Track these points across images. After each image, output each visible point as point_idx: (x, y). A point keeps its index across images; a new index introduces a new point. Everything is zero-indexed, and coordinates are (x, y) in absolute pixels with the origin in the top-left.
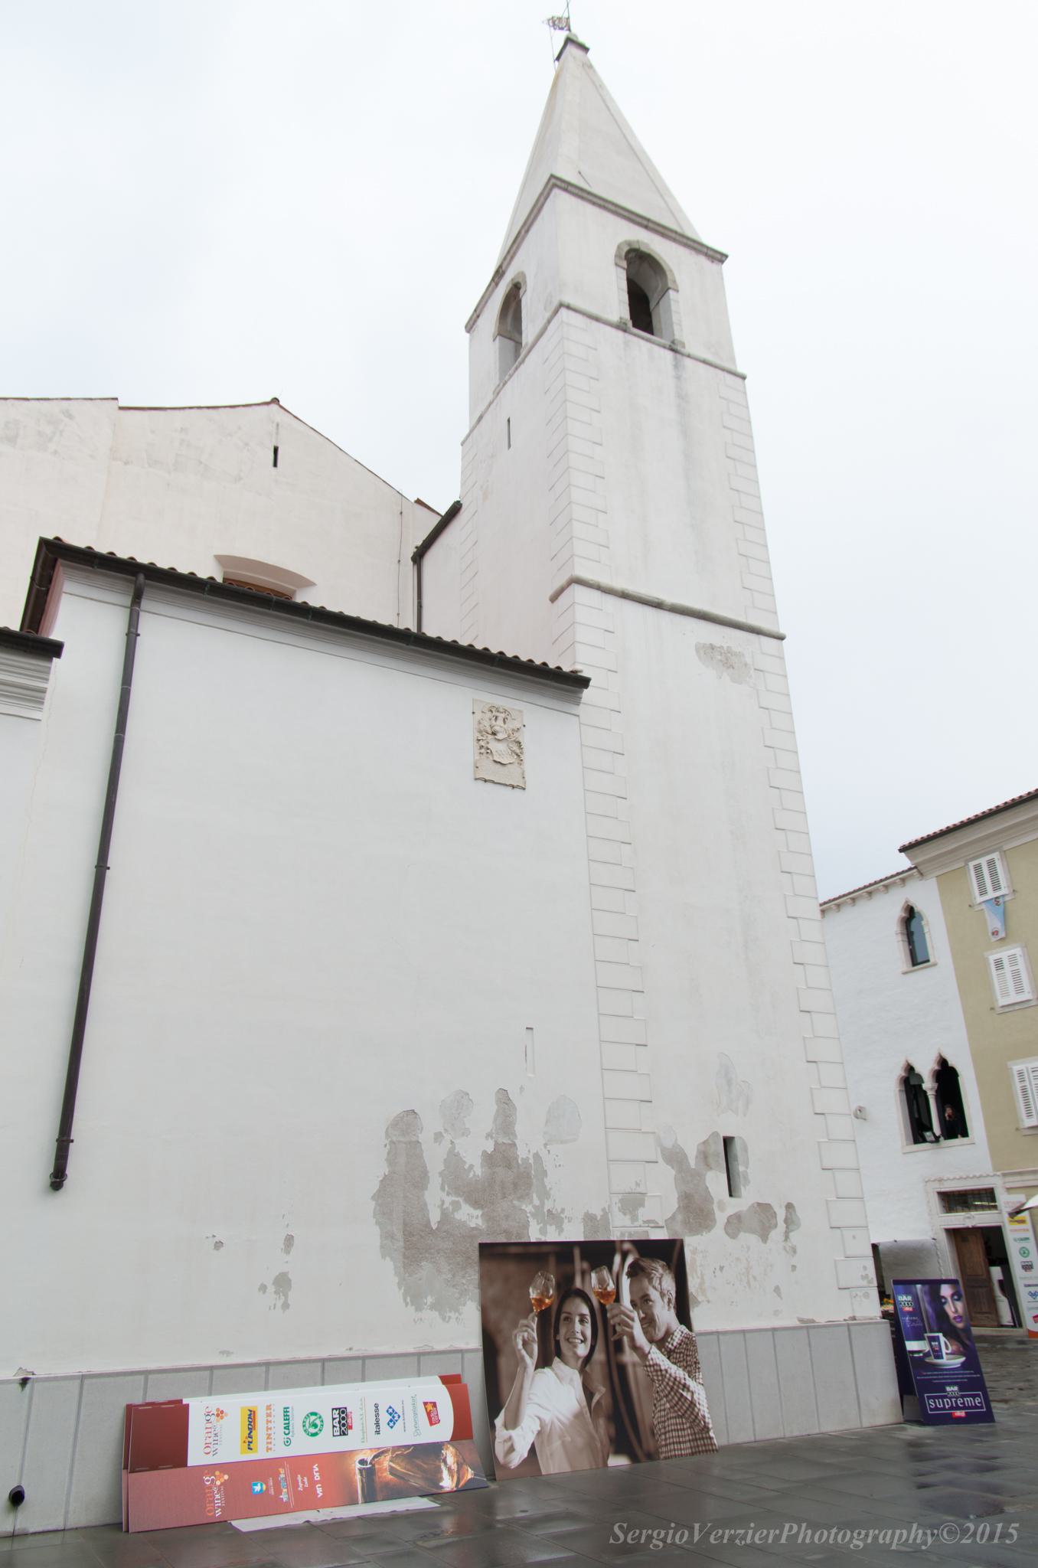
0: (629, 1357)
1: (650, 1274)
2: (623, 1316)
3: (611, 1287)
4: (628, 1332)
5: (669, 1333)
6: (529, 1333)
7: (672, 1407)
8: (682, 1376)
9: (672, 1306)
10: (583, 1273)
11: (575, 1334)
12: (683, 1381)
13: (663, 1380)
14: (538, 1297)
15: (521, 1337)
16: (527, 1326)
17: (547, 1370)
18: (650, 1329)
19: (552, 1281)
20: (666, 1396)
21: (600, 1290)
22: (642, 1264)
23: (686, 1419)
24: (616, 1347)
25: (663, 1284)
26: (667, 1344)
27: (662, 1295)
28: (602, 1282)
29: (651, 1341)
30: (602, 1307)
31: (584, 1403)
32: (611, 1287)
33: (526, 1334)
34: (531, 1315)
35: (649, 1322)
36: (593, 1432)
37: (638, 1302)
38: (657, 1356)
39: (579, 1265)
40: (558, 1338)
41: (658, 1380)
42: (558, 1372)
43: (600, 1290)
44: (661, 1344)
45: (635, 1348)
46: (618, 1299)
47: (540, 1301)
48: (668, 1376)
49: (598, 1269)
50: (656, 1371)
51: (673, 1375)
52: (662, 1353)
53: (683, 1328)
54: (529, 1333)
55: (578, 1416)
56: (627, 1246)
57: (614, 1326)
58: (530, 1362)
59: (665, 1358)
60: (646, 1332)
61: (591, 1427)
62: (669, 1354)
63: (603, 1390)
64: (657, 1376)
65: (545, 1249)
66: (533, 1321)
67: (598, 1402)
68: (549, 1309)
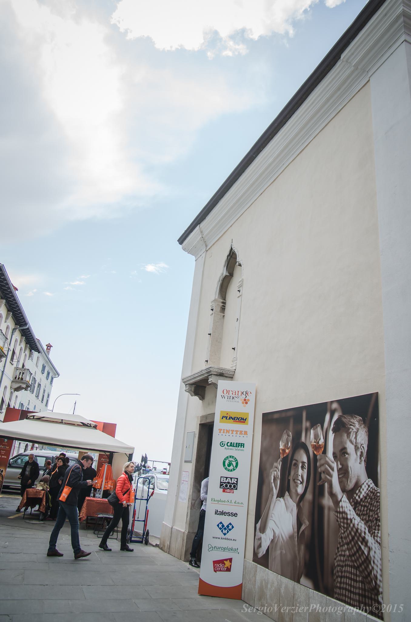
0: (327, 501)
1: (349, 429)
2: (327, 466)
3: (322, 441)
4: (328, 479)
5: (358, 486)
6: (277, 472)
7: (350, 556)
8: (363, 529)
9: (363, 459)
10: (307, 430)
11: (298, 477)
12: (363, 534)
13: (347, 528)
15: (273, 475)
16: (276, 468)
17: (281, 499)
18: (344, 479)
19: (290, 437)
20: (348, 544)
21: (315, 444)
22: (344, 420)
23: (360, 572)
24: (319, 492)
25: (358, 438)
26: (355, 495)
27: (356, 448)
28: (316, 437)
29: (343, 490)
30: (315, 456)
31: (296, 530)
32: (322, 441)
33: (276, 472)
34: (279, 460)
35: (344, 472)
36: (297, 552)
37: (338, 454)
38: (346, 505)
39: (305, 424)
40: (289, 479)
42: (286, 502)
43: (315, 444)
44: (350, 493)
45: (332, 495)
46: (325, 452)
47: (284, 451)
48: (352, 525)
49: (315, 427)
50: (344, 518)
51: (356, 526)
52: (351, 503)
53: (370, 481)
54: (277, 472)
55: (291, 537)
56: (335, 406)
57: (320, 473)
58: (275, 492)
59: (351, 508)
60: (341, 482)
61: (296, 549)
62: (356, 505)
63: (307, 523)
64: (344, 523)
65: (289, 414)
66: (279, 464)
67: (303, 531)
68: (287, 456)
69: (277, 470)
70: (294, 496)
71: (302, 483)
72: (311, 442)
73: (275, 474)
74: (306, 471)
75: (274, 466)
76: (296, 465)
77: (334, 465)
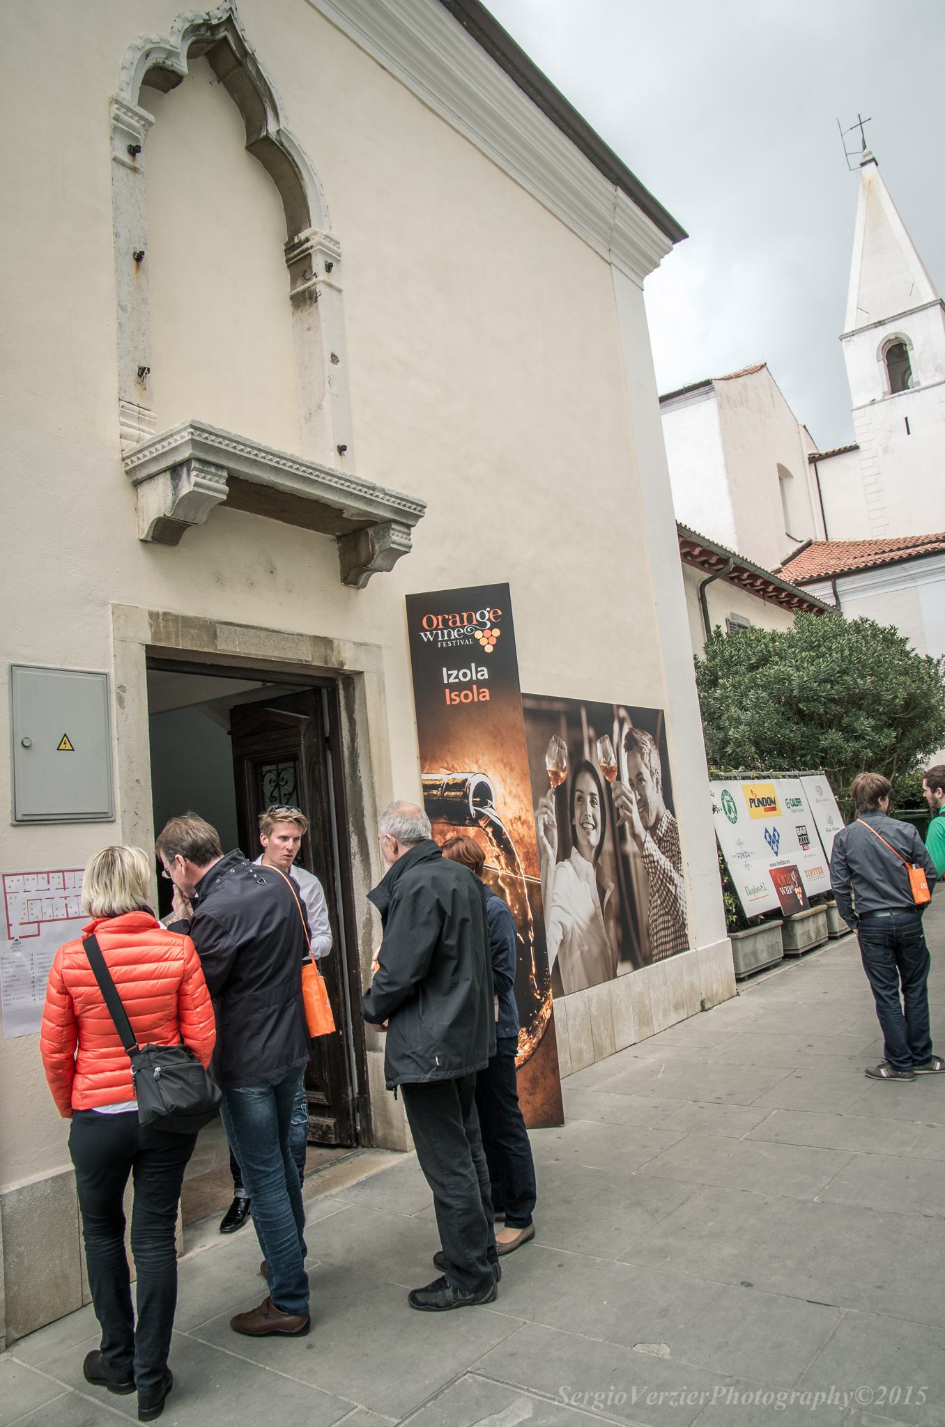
0: (631, 847)
1: (642, 748)
3: (613, 762)
5: (658, 819)
6: (549, 816)
7: (662, 903)
8: (669, 868)
9: (659, 786)
10: (591, 742)
12: (669, 874)
13: (655, 873)
14: (554, 770)
15: (542, 821)
16: (546, 806)
17: (566, 863)
20: (658, 891)
22: (636, 735)
23: (671, 915)
24: (619, 836)
25: (652, 760)
27: (652, 774)
28: (606, 754)
29: (646, 828)
30: (608, 783)
31: (598, 904)
32: (613, 762)
33: (546, 816)
34: (550, 792)
35: (643, 804)
36: (605, 936)
37: (635, 781)
38: (651, 846)
39: (588, 732)
41: (652, 873)
42: (576, 864)
44: (652, 829)
45: (635, 836)
46: (619, 778)
47: (556, 774)
49: (602, 738)
50: (651, 862)
51: (663, 867)
53: (668, 812)
54: (549, 816)
55: (594, 919)
56: (622, 713)
57: (618, 809)
58: (552, 852)
59: (656, 847)
61: (604, 931)
62: (659, 842)
63: (612, 885)
64: (651, 868)
65: (557, 706)
66: (551, 800)
68: (564, 784)
69: (549, 812)
70: (586, 850)
71: (595, 827)
72: (599, 762)
73: (546, 820)
74: (598, 807)
75: (540, 804)
76: (581, 798)
77: (632, 796)
